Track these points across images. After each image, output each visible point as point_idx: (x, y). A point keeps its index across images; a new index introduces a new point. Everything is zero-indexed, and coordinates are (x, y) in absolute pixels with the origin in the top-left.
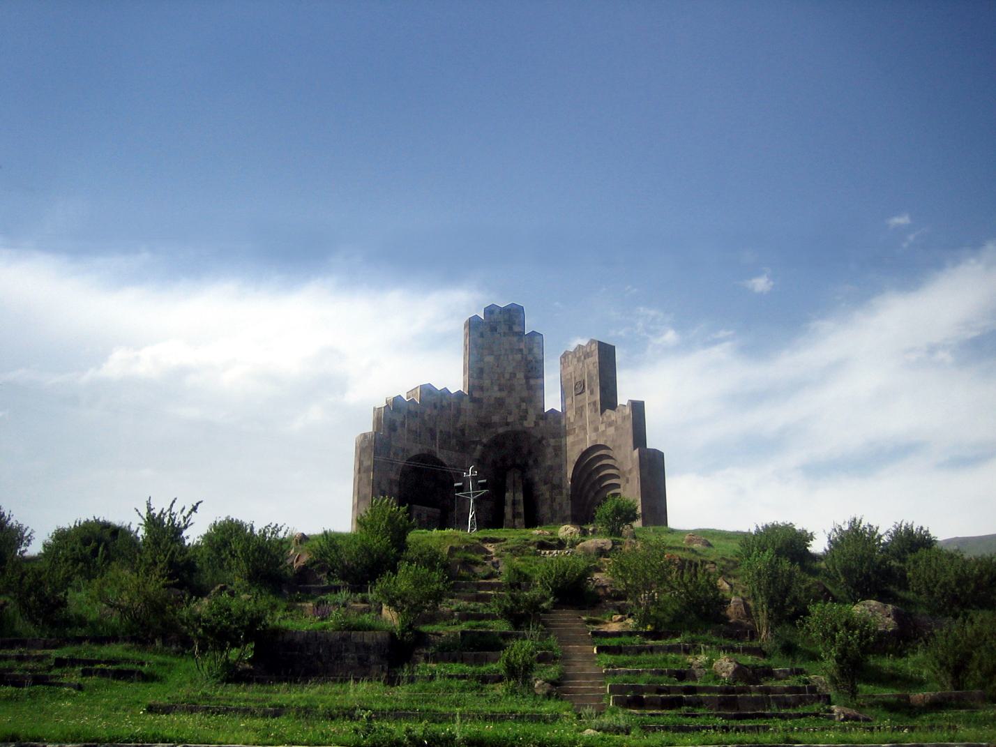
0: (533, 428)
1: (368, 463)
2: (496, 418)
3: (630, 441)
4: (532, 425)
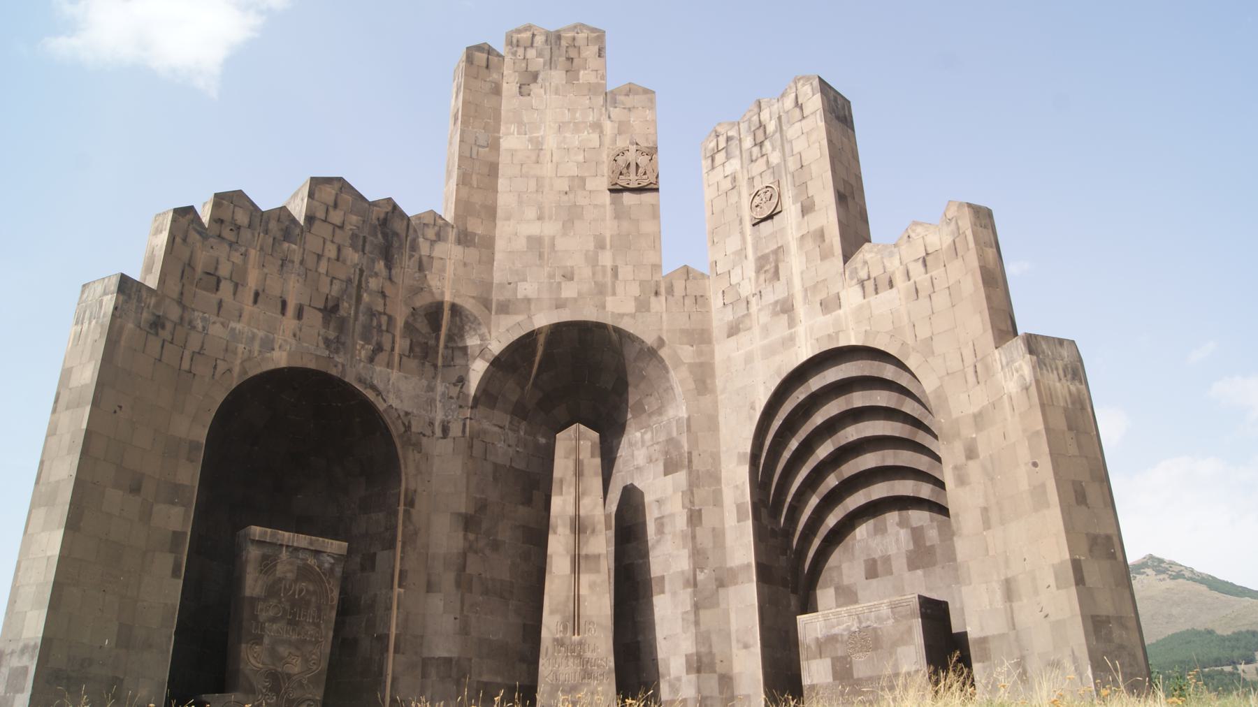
0: (633, 316)
1: (87, 375)
2: (527, 289)
3: (977, 324)
4: (630, 307)
